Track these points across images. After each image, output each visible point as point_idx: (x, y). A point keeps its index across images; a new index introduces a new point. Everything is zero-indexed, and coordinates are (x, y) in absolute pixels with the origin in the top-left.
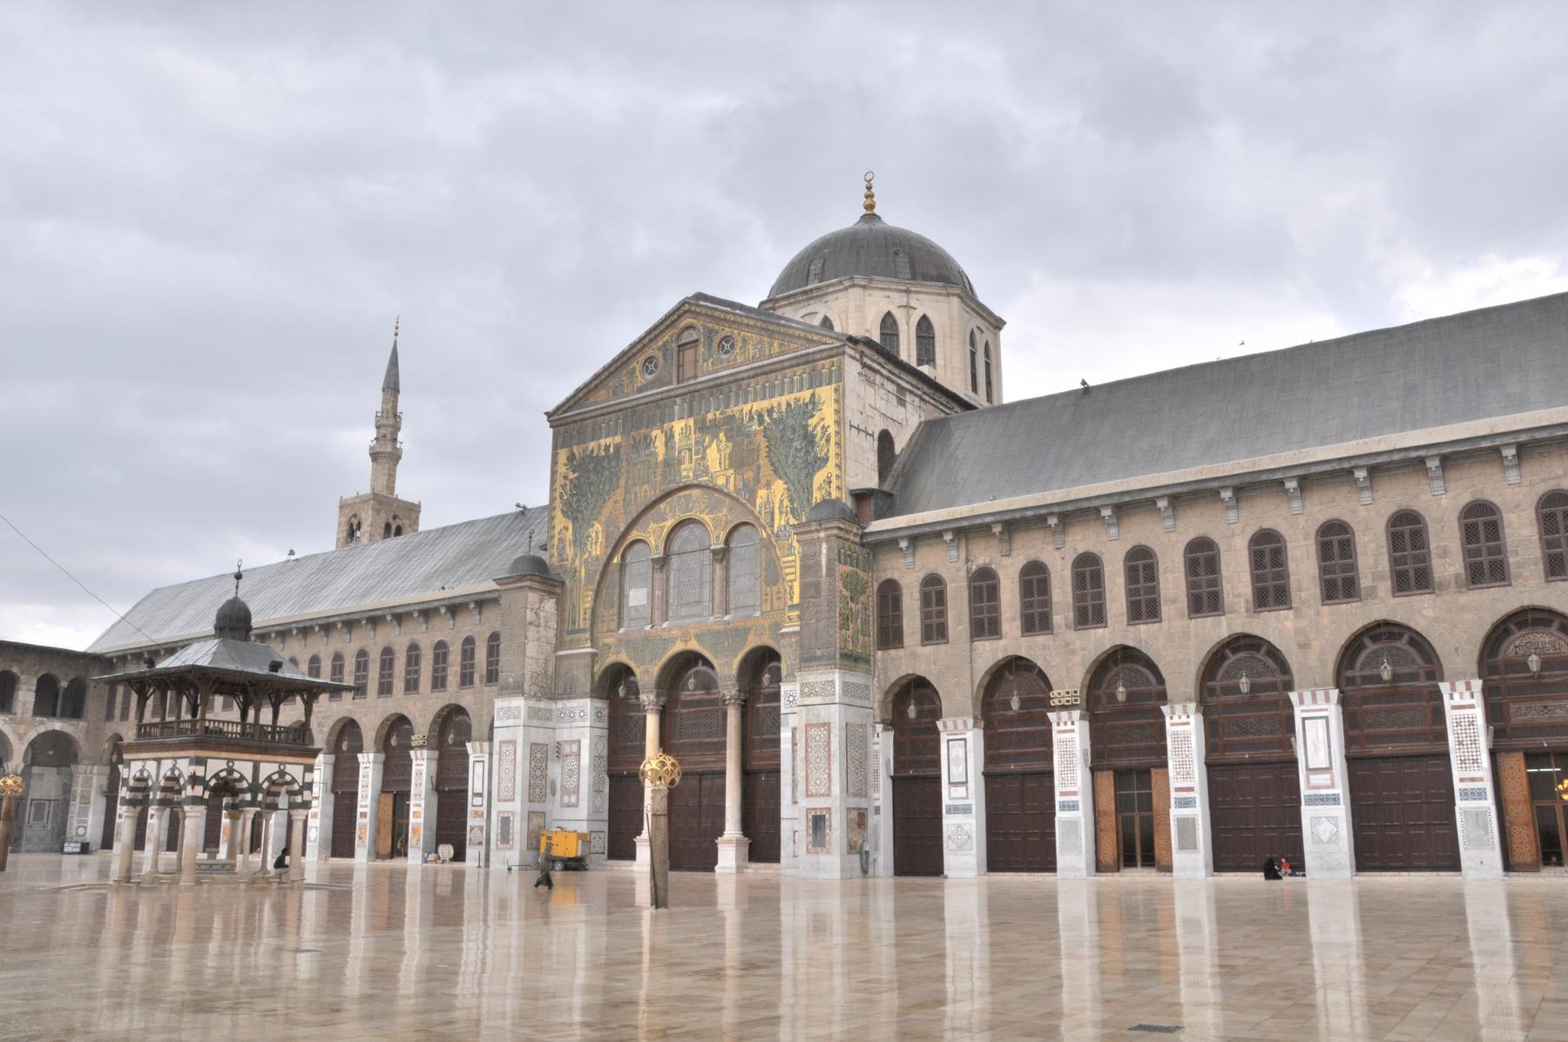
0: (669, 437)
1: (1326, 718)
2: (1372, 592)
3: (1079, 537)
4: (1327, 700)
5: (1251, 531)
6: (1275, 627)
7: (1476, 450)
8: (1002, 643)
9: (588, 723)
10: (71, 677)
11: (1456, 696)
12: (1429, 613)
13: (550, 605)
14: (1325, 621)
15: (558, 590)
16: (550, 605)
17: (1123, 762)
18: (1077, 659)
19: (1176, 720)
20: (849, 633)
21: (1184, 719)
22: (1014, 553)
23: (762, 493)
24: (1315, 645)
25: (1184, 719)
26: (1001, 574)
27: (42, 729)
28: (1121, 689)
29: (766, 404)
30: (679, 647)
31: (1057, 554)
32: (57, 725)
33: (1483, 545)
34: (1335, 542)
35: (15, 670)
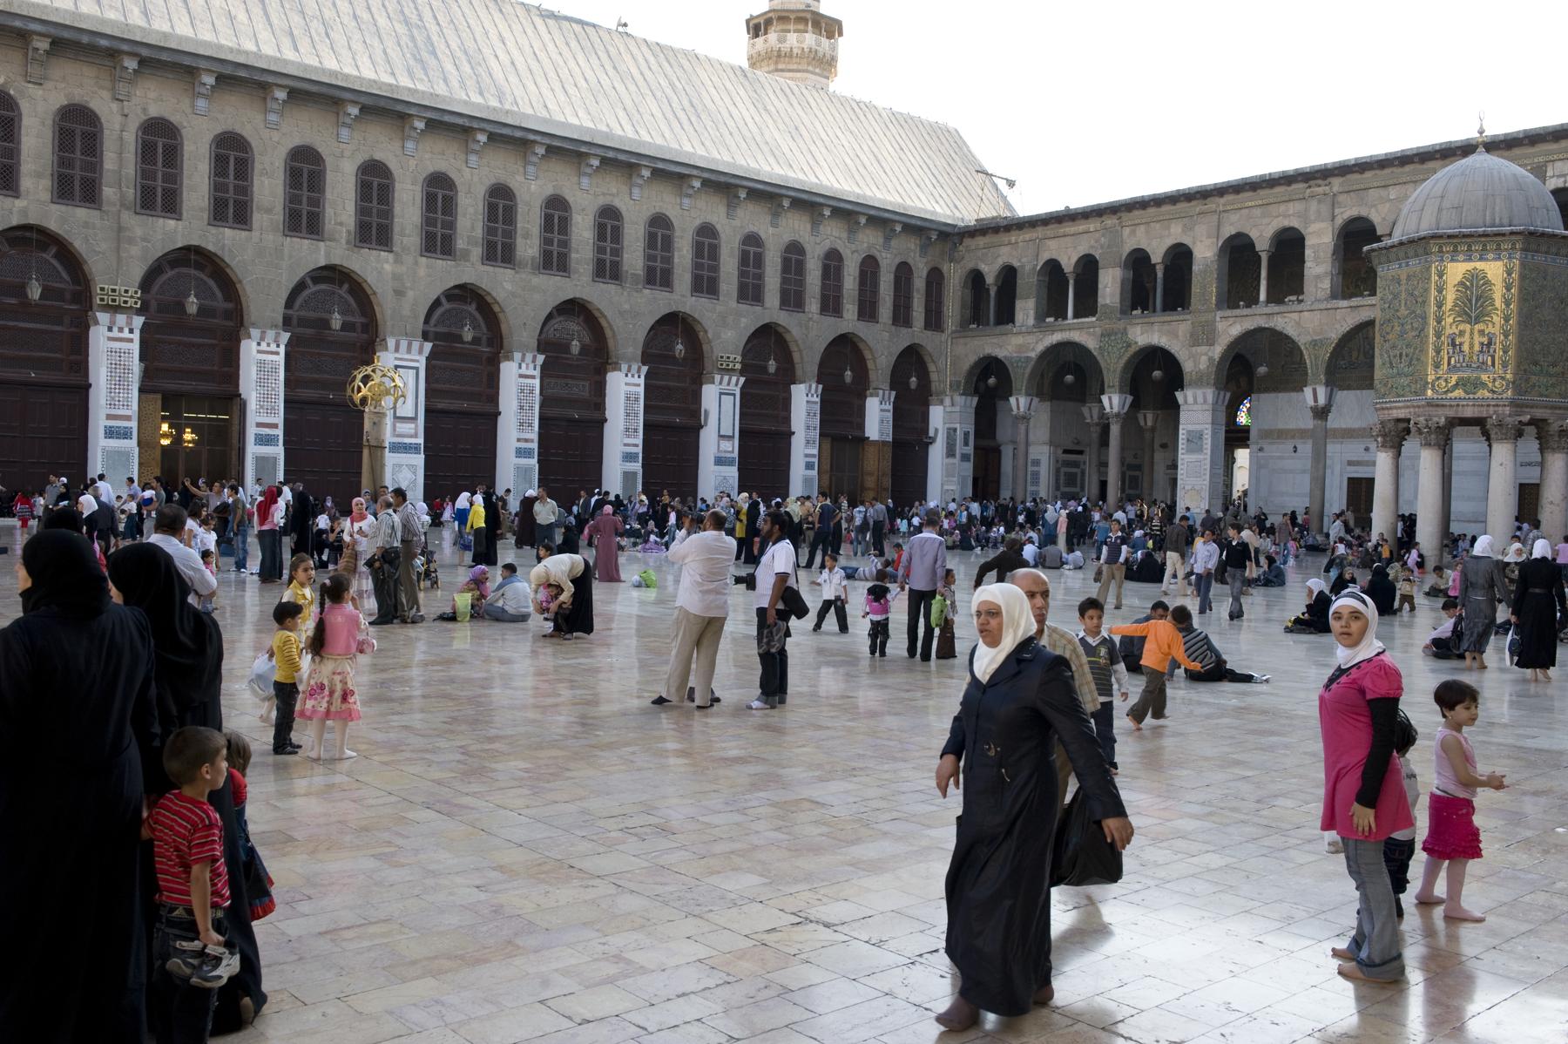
2: (466, 255)
3: (152, 95)
4: (420, 352)
5: (360, 159)
6: (374, 267)
7: (441, 122)
8: (19, 203)
14: (422, 272)
17: (172, 386)
18: (135, 251)
19: (264, 346)
21: (273, 347)
22: (49, 85)
24: (410, 294)
25: (273, 347)
26: (24, 106)
28: (192, 299)
31: (115, 106)
33: (556, 237)
34: (305, 169)
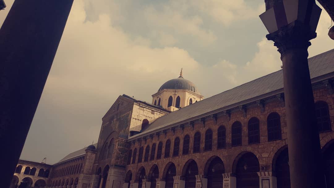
0: (114, 122)
1: (178, 183)
9: (94, 179)
10: (46, 169)
11: (198, 179)
12: (198, 157)
13: (94, 155)
15: (96, 153)
16: (94, 155)
20: (119, 161)
23: (120, 132)
24: (180, 165)
27: (39, 179)
29: (124, 115)
30: (107, 164)
32: (42, 178)
35: (36, 167)
